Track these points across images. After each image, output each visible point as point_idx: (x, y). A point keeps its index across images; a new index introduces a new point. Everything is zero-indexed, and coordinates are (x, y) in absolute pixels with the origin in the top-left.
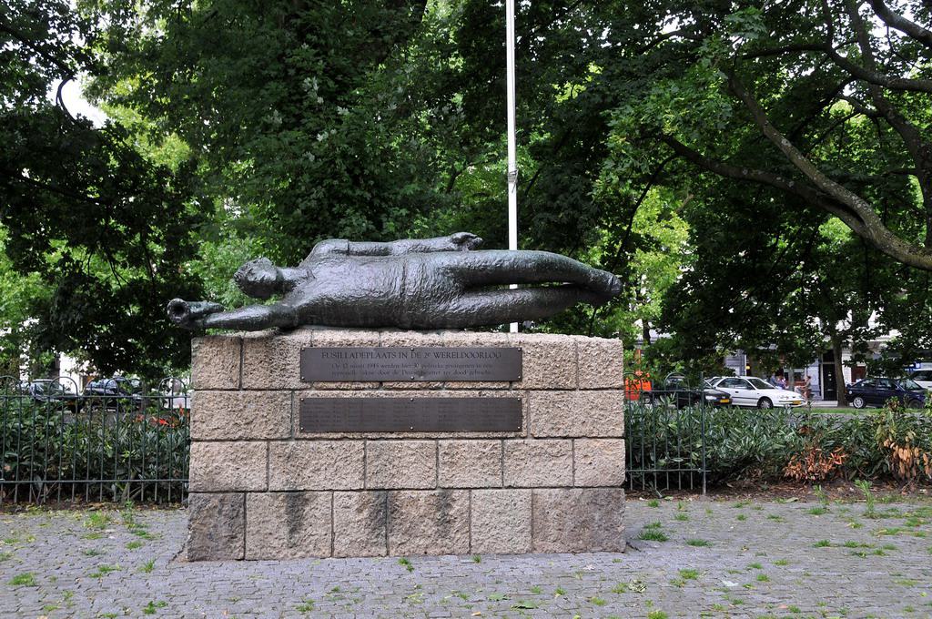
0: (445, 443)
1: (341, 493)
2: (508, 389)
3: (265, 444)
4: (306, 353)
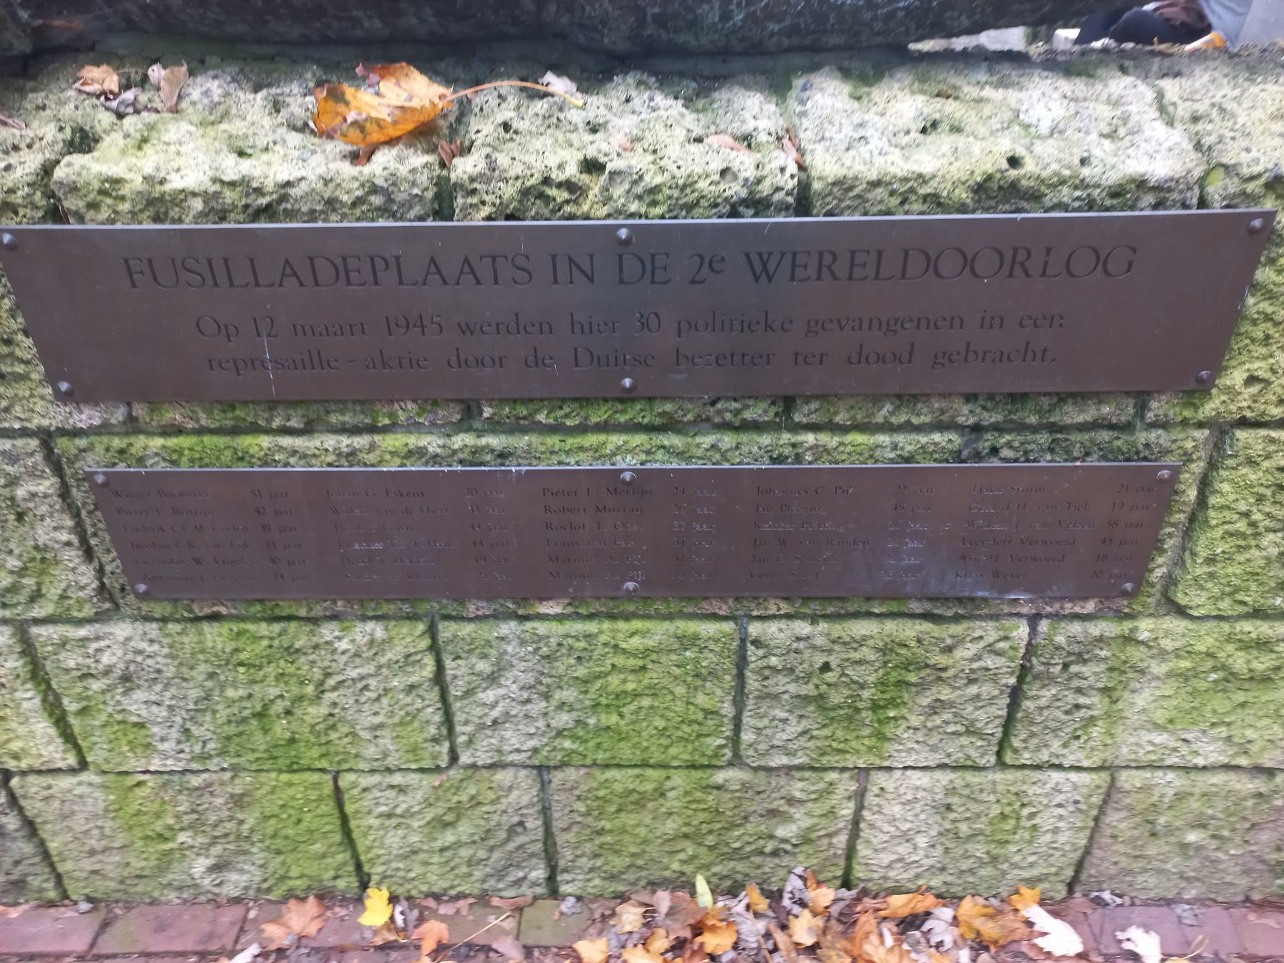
0: (774, 631)
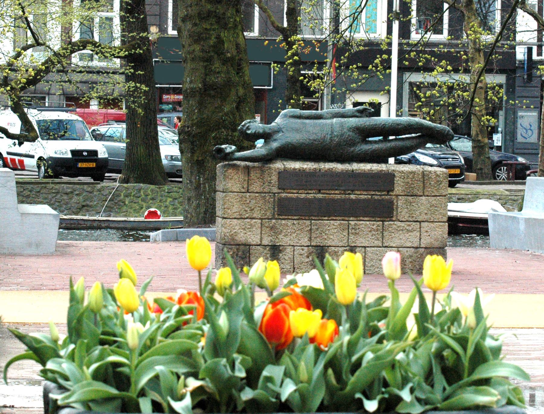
0: (352, 223)
1: (299, 248)
2: (386, 195)
3: (260, 221)
4: (283, 174)
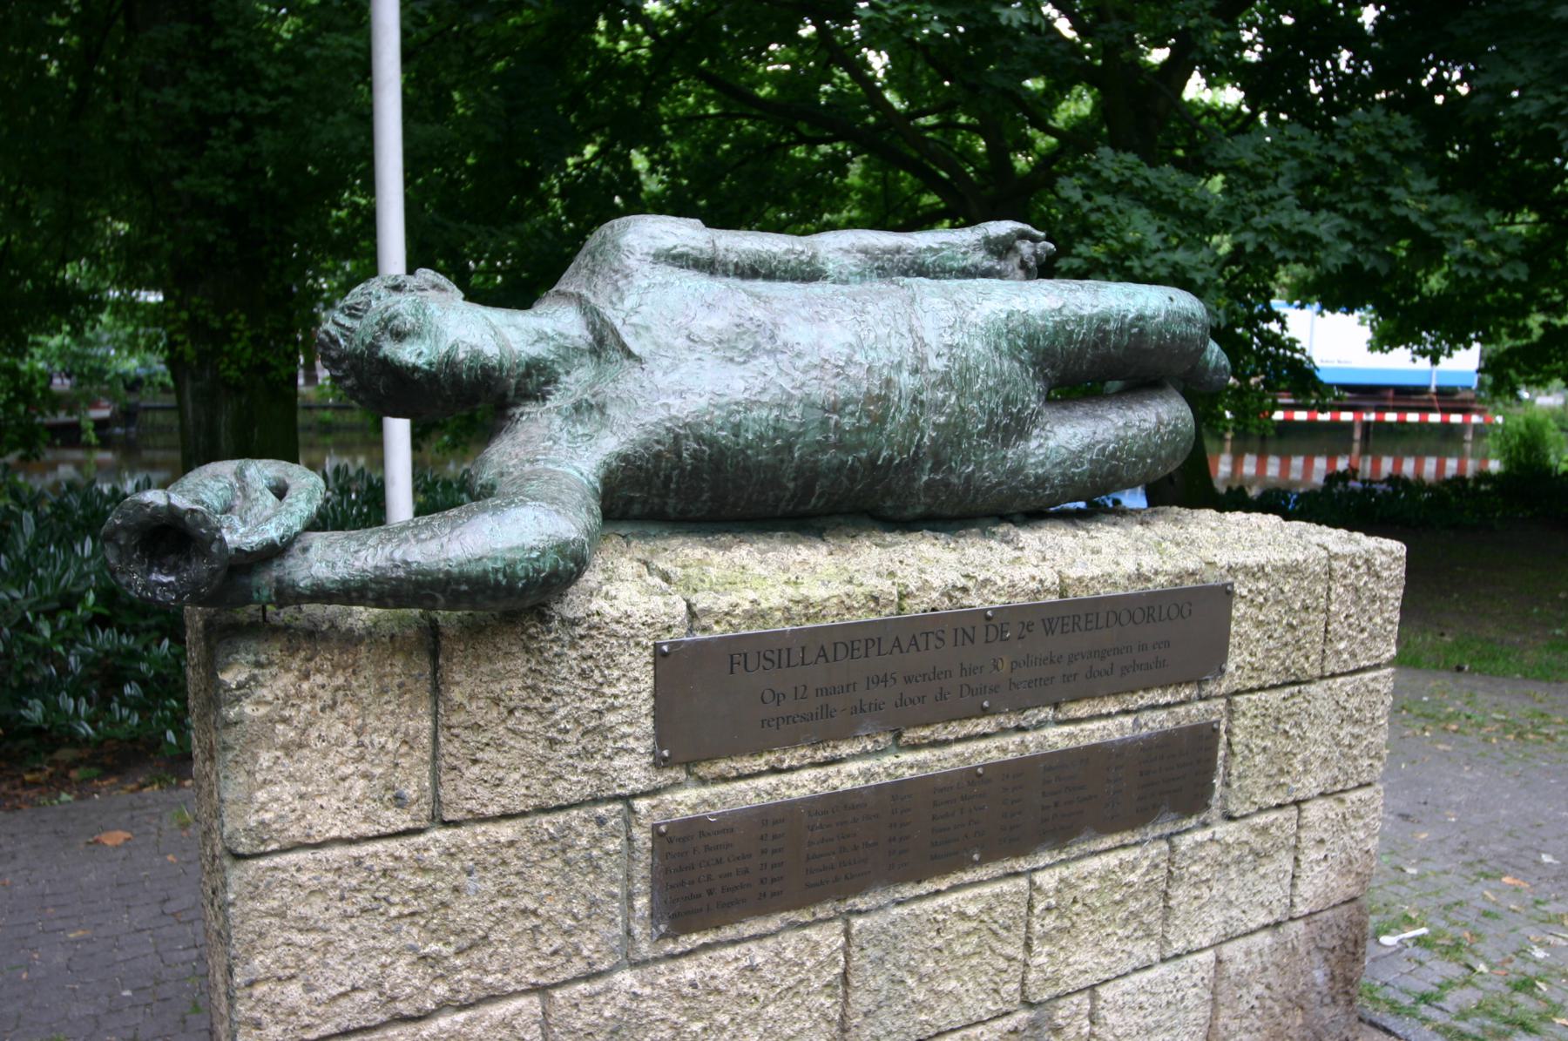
0: (1047, 880)
3: (532, 1005)
